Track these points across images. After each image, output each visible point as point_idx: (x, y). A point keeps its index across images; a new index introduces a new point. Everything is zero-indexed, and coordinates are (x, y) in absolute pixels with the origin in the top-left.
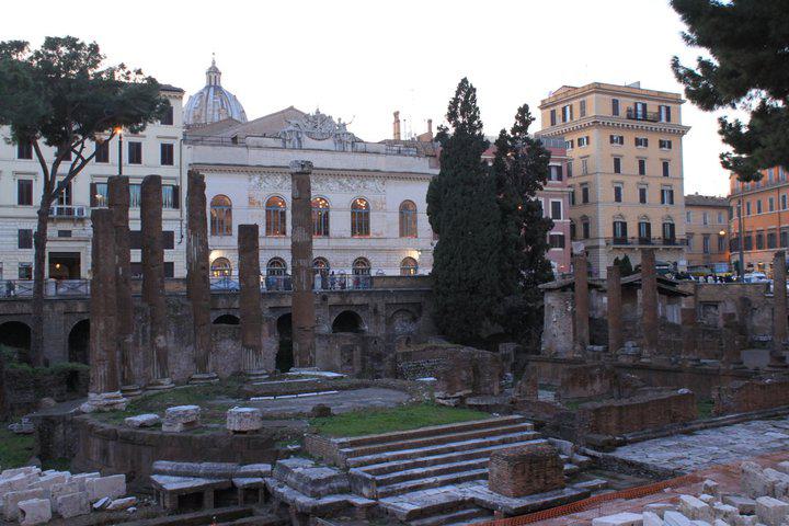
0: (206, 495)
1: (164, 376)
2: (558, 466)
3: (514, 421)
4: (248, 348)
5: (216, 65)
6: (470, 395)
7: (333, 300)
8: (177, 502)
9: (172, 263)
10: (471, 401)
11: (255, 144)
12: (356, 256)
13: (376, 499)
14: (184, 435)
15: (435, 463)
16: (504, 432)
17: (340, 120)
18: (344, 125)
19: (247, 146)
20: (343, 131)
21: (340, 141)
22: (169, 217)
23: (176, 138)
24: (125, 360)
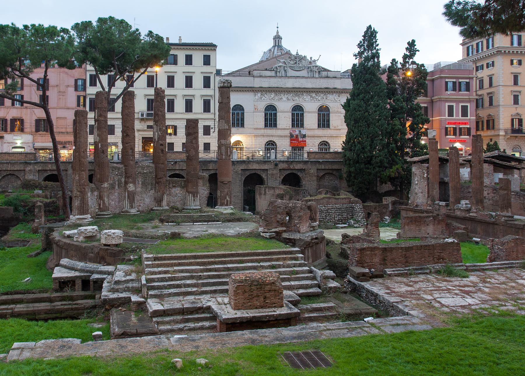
0: (77, 282)
1: (132, 207)
2: (278, 293)
3: (291, 253)
4: (189, 192)
5: (279, 34)
6: (285, 231)
7: (281, 166)
8: (58, 285)
9: (204, 143)
10: (285, 235)
11: (258, 75)
12: (267, 139)
13: (146, 299)
14: (84, 245)
15: (209, 277)
16: (278, 260)
17: (311, 58)
18: (315, 61)
19: (253, 76)
20: (314, 65)
21: (311, 71)
22: (169, 117)
23: (212, 73)
24: (100, 197)
